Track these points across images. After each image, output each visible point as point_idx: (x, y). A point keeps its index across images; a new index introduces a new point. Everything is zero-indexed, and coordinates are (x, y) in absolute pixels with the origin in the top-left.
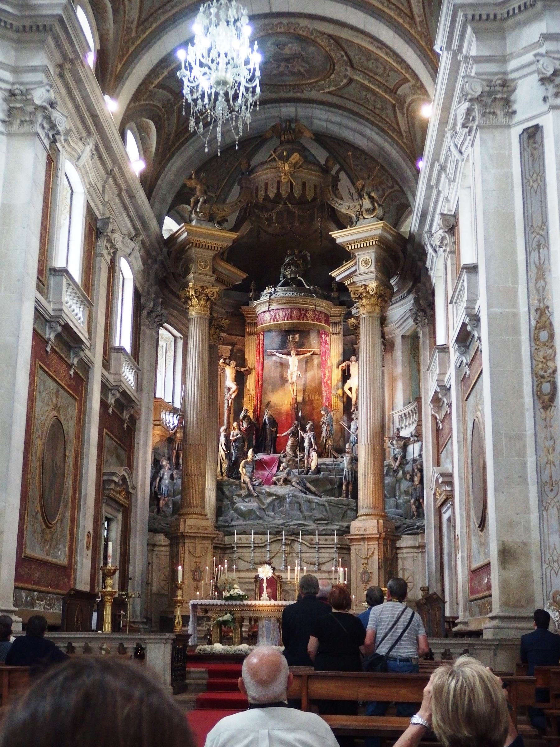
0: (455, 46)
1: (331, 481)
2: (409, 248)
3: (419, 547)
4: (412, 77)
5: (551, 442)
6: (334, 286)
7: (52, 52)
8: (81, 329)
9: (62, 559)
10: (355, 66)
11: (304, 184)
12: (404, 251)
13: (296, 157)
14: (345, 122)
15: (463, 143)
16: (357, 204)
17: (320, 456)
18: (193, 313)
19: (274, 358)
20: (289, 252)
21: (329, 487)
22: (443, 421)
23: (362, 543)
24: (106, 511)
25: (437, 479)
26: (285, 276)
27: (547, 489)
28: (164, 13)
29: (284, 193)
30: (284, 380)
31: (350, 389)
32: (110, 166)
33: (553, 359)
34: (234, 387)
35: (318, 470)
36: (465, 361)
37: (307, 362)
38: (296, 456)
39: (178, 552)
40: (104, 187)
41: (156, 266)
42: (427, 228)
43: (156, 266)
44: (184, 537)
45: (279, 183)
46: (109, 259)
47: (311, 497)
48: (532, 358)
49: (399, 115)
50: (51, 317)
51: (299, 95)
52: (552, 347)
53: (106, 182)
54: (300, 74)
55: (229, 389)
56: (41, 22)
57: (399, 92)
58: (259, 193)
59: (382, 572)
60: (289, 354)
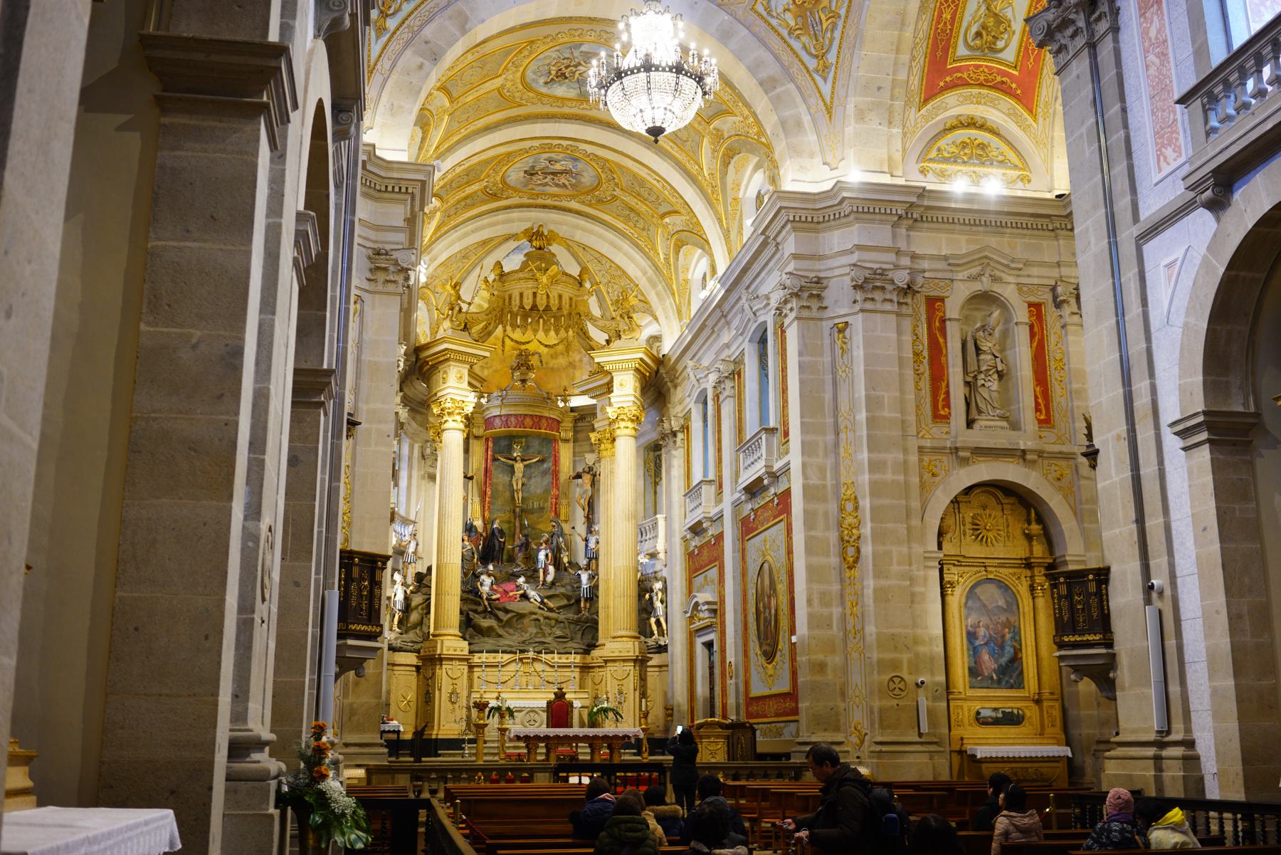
3: (660, 666)
11: (560, 296)
23: (617, 664)
25: (697, 604)
39: (434, 674)
45: (535, 294)
51: (557, 203)
54: (564, 186)
57: (667, 220)
58: (513, 303)
59: (637, 693)
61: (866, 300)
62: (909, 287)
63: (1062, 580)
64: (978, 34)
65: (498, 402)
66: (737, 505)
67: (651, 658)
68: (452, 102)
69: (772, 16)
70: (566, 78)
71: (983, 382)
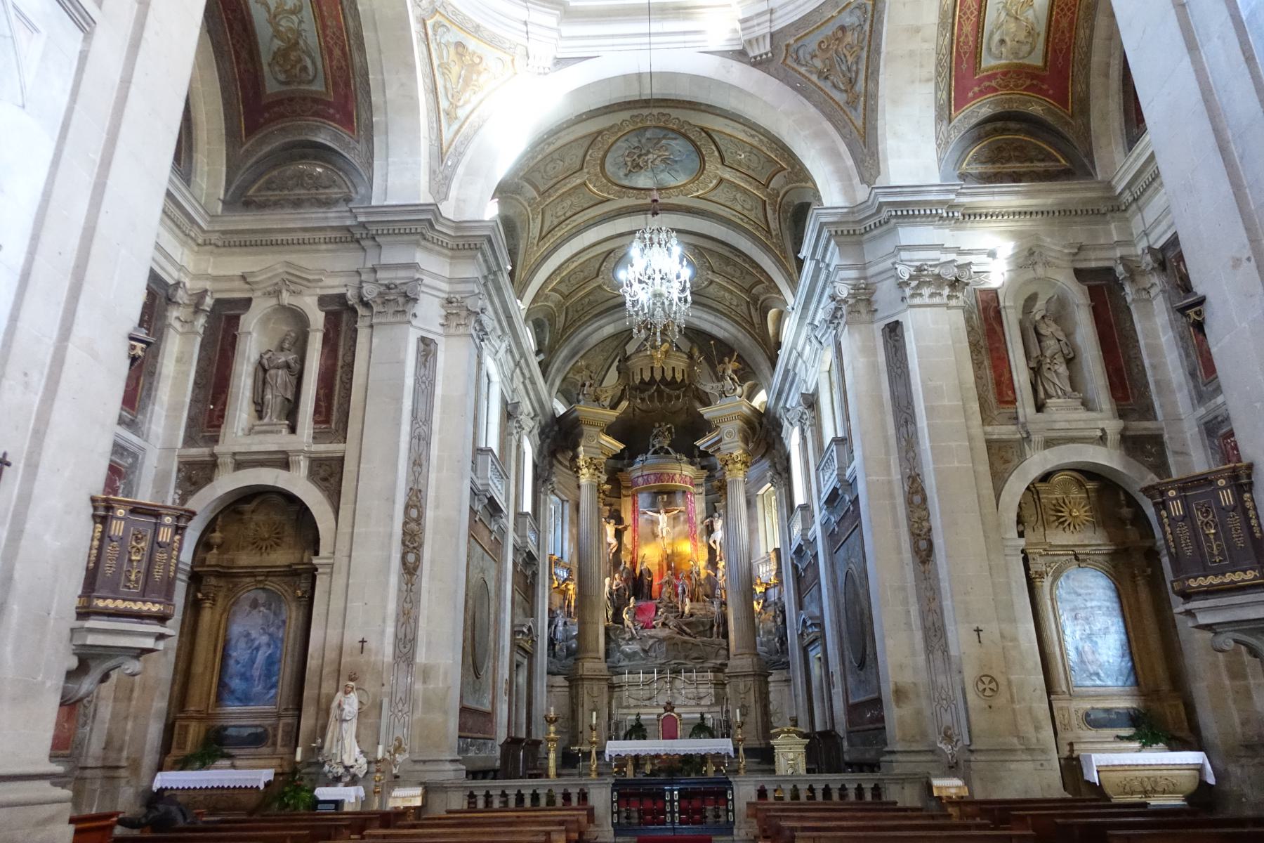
0: (819, 256)
1: (703, 624)
2: (765, 420)
4: (767, 280)
5: (932, 593)
6: (696, 453)
7: (479, 265)
8: (501, 500)
10: (715, 270)
11: (673, 368)
12: (761, 424)
14: (705, 316)
15: (823, 335)
16: (719, 385)
17: (691, 600)
19: (646, 516)
20: (657, 425)
21: (701, 628)
22: (805, 570)
24: (518, 657)
25: (804, 622)
26: (653, 446)
27: (932, 633)
28: (559, 230)
29: (658, 377)
30: (655, 536)
31: (715, 542)
32: (517, 358)
33: (928, 520)
34: (614, 542)
35: (692, 615)
36: (833, 520)
37: (674, 519)
38: (671, 602)
39: (577, 693)
40: (512, 375)
41: (548, 441)
42: (781, 404)
43: (548, 441)
45: (652, 368)
46: (517, 437)
47: (687, 638)
48: (909, 518)
49: (753, 310)
50: (479, 490)
52: (926, 509)
53: (513, 372)
55: (610, 544)
59: (758, 705)
61: (913, 296)
62: (957, 280)
63: (1172, 493)
64: (1002, 41)
65: (641, 465)
66: (825, 525)
67: (771, 674)
68: (542, 194)
69: (803, 65)
70: (641, 168)
71: (1048, 366)
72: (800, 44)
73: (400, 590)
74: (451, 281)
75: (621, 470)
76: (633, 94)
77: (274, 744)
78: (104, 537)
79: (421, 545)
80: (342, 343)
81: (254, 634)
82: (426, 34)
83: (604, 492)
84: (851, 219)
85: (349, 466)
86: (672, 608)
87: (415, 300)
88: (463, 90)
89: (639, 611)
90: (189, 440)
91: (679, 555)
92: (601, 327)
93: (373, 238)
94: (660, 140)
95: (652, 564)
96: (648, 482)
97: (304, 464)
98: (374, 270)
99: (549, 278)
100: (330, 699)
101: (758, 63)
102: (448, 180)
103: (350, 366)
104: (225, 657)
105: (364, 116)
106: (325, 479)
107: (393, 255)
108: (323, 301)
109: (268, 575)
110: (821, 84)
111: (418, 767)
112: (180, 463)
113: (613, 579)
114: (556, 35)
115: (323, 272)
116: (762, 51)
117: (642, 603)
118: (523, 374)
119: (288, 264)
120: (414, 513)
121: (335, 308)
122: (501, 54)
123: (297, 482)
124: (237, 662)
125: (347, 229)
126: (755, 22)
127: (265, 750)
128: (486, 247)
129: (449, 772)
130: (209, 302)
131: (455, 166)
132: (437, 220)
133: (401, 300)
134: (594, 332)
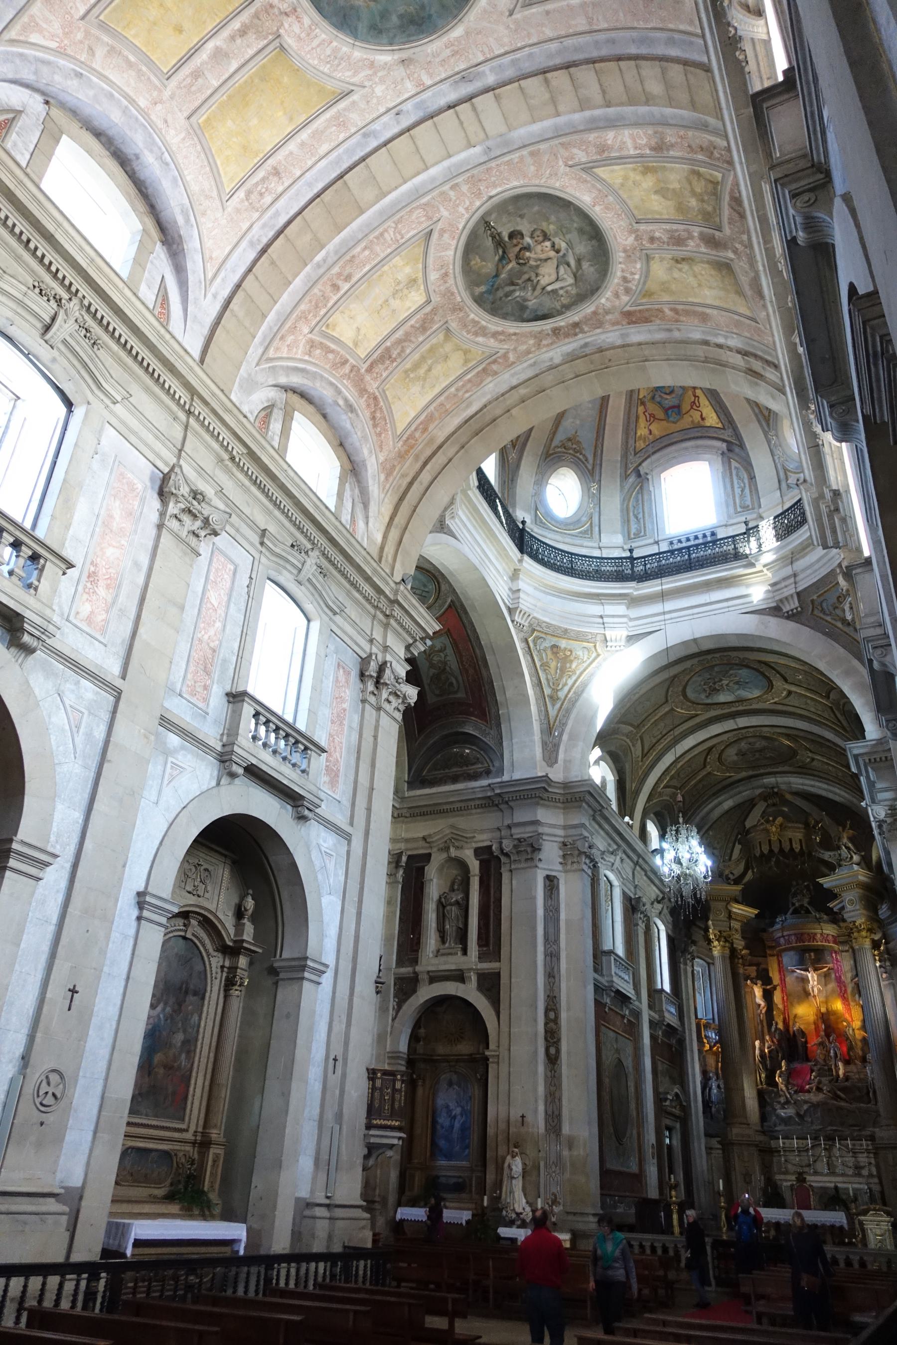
8: (628, 989)
9: (634, 1169)
13: (780, 820)
18: (716, 952)
26: (793, 904)
29: (776, 850)
30: (807, 994)
34: (763, 1004)
35: (847, 1078)
44: (733, 1144)
45: (770, 841)
46: (643, 926)
47: (843, 1104)
56: (577, 796)
60: (806, 970)
72: (822, 598)
73: (546, 1076)
74: (565, 827)
75: (764, 930)
76: (694, 650)
77: (471, 1192)
78: (373, 1089)
79: (559, 1040)
80: (492, 884)
81: (452, 1105)
82: (529, 648)
83: (742, 957)
84: (880, 748)
85: (504, 980)
86: (827, 1070)
87: (540, 850)
88: (561, 677)
89: (790, 1076)
90: (400, 962)
91: (834, 1013)
92: (720, 803)
93: (507, 803)
94: (727, 672)
95: (808, 1024)
96: (789, 942)
97: (474, 978)
98: (509, 827)
99: (660, 779)
100: (504, 1159)
101: (791, 616)
102: (556, 747)
103: (499, 900)
104: (434, 1122)
105: (493, 711)
106: (488, 990)
107: (521, 815)
108: (478, 852)
109: (457, 1061)
110: (846, 629)
111: (570, 1217)
112: (395, 979)
113: (763, 1042)
114: (625, 620)
115: (475, 831)
116: (793, 606)
117: (796, 1065)
118: (642, 869)
119: (452, 826)
120: (552, 1015)
121: (485, 857)
122: (585, 644)
123: (470, 992)
124: (442, 1127)
125: (489, 797)
126: (783, 584)
127: (464, 1195)
128: (588, 797)
129: (590, 1224)
130: (404, 859)
131: (561, 735)
132: (549, 785)
133: (529, 849)
134: (716, 806)
